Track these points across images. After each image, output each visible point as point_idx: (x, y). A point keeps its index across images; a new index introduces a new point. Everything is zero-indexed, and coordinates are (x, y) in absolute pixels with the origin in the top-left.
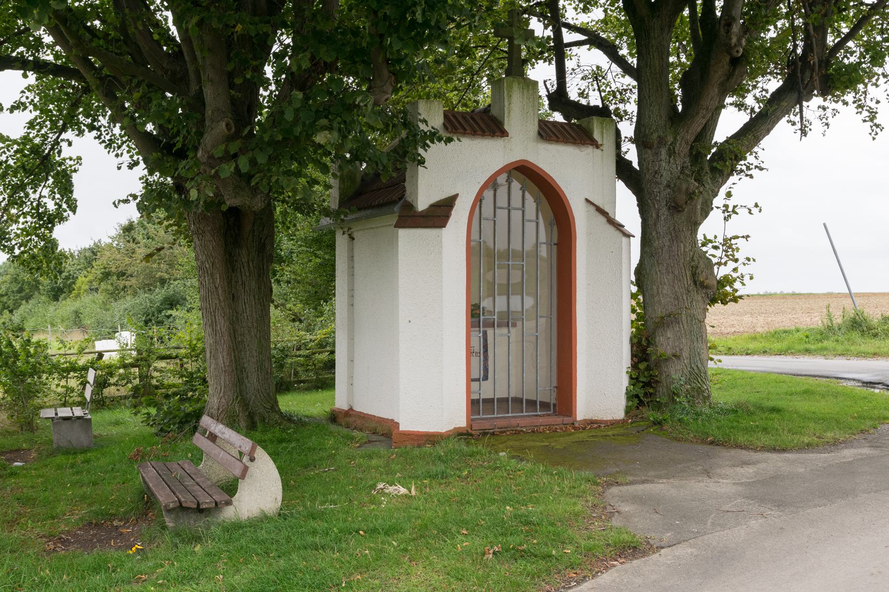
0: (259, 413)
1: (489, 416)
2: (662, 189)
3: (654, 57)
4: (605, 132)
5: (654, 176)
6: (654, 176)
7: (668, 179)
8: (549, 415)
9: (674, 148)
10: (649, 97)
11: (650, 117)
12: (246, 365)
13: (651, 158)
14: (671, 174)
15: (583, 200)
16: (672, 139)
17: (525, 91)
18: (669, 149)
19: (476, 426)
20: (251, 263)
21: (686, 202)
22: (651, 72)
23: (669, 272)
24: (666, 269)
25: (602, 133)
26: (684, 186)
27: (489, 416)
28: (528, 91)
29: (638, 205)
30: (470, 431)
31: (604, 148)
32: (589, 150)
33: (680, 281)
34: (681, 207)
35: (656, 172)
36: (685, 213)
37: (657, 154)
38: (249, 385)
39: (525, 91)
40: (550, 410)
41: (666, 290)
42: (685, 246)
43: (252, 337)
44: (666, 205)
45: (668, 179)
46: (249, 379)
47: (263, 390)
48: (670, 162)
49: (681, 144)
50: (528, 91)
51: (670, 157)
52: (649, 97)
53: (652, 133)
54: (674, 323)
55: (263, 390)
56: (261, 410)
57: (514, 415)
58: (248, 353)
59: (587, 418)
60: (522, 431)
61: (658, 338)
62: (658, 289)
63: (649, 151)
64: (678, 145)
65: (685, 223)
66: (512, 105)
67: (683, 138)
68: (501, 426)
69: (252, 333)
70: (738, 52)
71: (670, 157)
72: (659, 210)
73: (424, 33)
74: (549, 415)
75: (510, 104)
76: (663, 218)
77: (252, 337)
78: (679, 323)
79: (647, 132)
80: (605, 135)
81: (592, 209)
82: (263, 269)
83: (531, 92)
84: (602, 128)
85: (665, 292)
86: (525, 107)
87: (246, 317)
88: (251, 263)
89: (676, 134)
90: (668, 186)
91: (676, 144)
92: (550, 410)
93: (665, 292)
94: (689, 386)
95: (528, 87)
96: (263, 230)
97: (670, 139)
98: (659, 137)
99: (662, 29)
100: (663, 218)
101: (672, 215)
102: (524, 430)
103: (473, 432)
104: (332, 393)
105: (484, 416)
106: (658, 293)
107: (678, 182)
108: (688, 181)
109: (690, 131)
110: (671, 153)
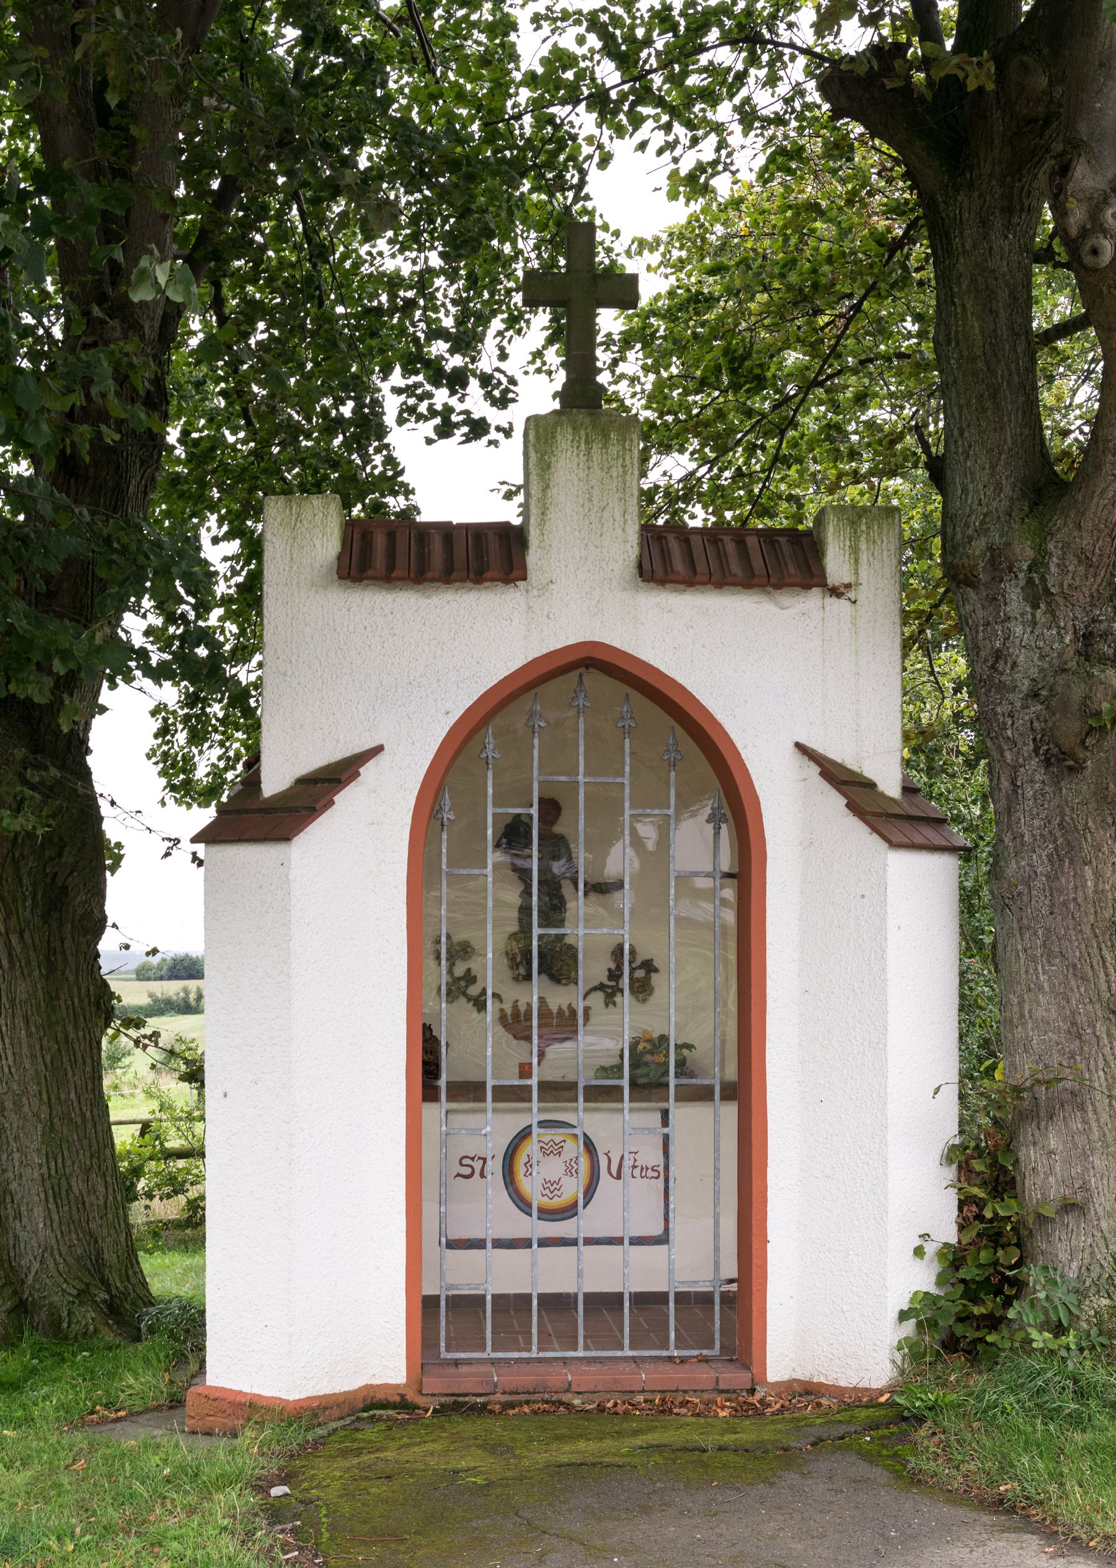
0: (51, 1304)
1: (516, 1355)
2: (1018, 704)
3: (964, 309)
4: (863, 546)
5: (993, 667)
6: (993, 667)
7: (1034, 672)
8: (705, 1360)
9: (1043, 579)
10: (961, 434)
11: (965, 491)
12: (14, 1186)
13: (980, 613)
14: (1042, 657)
15: (790, 746)
16: (1030, 553)
17: (596, 449)
18: (1030, 581)
19: (433, 1384)
20: (14, 939)
21: (1083, 742)
22: (961, 357)
23: (1050, 956)
24: (1044, 945)
25: (855, 551)
26: (1077, 692)
27: (516, 1355)
28: (605, 447)
29: (88, 751)
30: (411, 1396)
31: (863, 594)
32: (812, 601)
33: (1084, 979)
34: (1072, 756)
35: (998, 655)
36: (1087, 773)
37: (994, 600)
38: (23, 1236)
39: (596, 449)
40: (710, 1345)
41: (1045, 1007)
42: (1098, 875)
43: (25, 1119)
44: (1036, 750)
45: (1034, 672)
46: (25, 1221)
47: (64, 1250)
48: (1034, 623)
49: (1062, 567)
50: (605, 447)
51: (1035, 606)
52: (961, 434)
53: (971, 539)
54: (1068, 1108)
55: (64, 1250)
56: (56, 1298)
57: (594, 1354)
58: (16, 1155)
59: (801, 1375)
60: (568, 1406)
61: (1024, 1149)
62: (1021, 1004)
63: (971, 593)
64: (1053, 569)
65: (1092, 806)
66: (553, 491)
67: (1066, 547)
68: (512, 1388)
69: (26, 1109)
70: (1095, 252)
71: (1035, 606)
72: (1015, 768)
73: (346, 316)
74: (705, 1360)
75: (546, 488)
76: (1029, 793)
77: (25, 1119)
78: (1083, 1109)
79: (959, 536)
80: (864, 557)
81: (815, 770)
82: (64, 952)
83: (614, 450)
84: (855, 536)
85: (1039, 1013)
86: (596, 492)
87: (6, 1070)
88: (14, 939)
89: (1043, 535)
90: (1035, 695)
91: (1047, 566)
92: (710, 1345)
93: (1039, 1013)
94: (1105, 1302)
95: (606, 436)
96: (60, 855)
97: (1024, 552)
98: (990, 548)
99: (983, 222)
100: (1029, 793)
101: (1056, 781)
102: (577, 1402)
103: (421, 1401)
104: (196, 1260)
105: (542, 1355)
106: (1022, 1016)
107: (1061, 680)
108: (1091, 676)
109: (1088, 524)
110: (1036, 594)
